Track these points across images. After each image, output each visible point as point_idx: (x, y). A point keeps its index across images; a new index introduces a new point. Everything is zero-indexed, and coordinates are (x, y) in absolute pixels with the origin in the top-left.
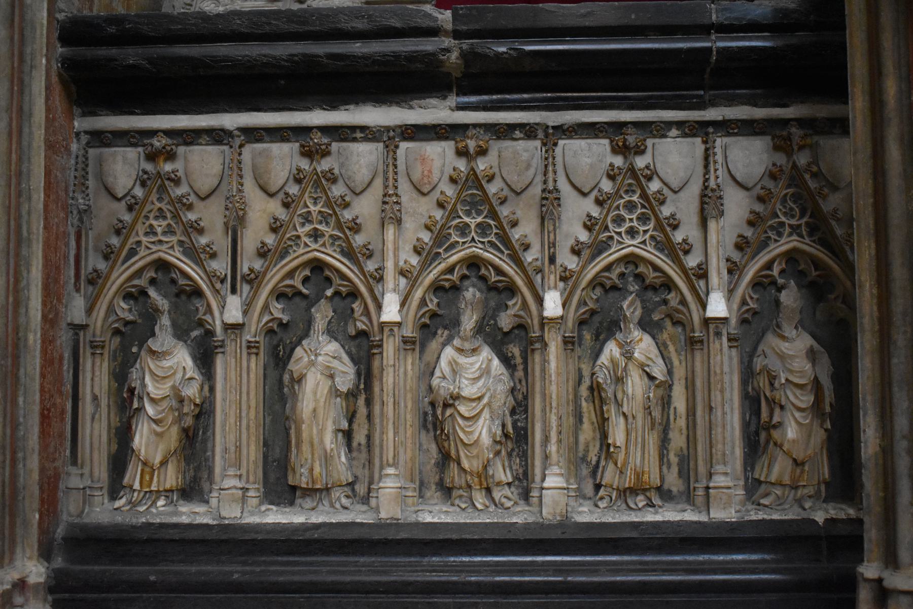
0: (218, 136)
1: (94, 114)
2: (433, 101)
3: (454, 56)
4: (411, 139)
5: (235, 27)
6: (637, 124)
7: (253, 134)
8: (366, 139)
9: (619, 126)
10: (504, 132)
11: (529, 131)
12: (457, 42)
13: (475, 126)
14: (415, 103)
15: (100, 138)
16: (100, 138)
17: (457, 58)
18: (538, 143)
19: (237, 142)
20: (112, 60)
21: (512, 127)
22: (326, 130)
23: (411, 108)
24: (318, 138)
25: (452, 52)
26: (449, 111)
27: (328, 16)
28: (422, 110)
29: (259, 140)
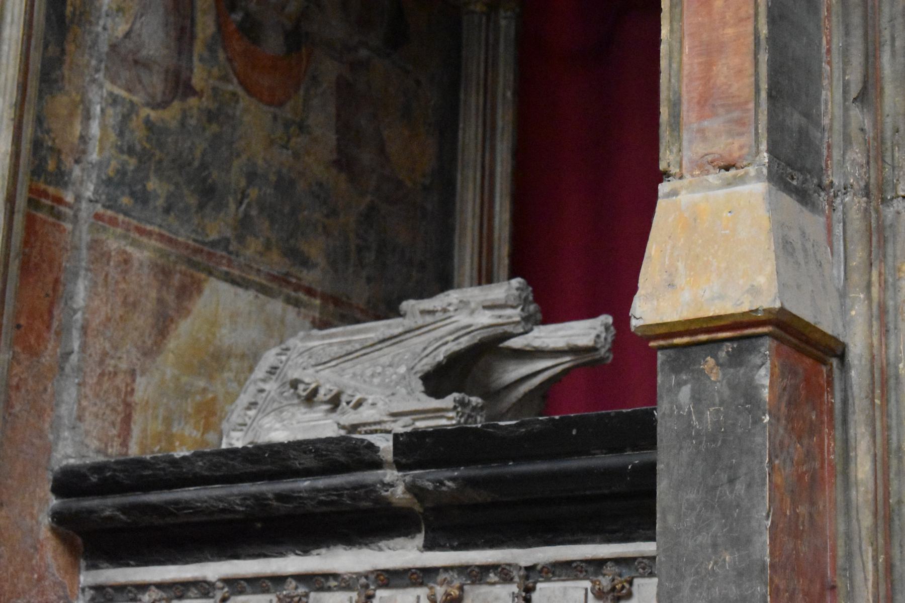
1: (95, 567)
2: (400, 541)
3: (400, 490)
4: (386, 585)
5: (197, 470)
6: (620, 561)
8: (340, 588)
9: (598, 564)
10: (478, 574)
11: (503, 573)
12: (401, 474)
13: (446, 569)
14: (382, 544)
17: (404, 493)
18: (514, 588)
19: (219, 595)
20: (91, 511)
21: (485, 569)
22: (303, 578)
23: (380, 549)
25: (395, 484)
26: (418, 553)
27: (278, 452)
28: (391, 552)
29: (241, 592)
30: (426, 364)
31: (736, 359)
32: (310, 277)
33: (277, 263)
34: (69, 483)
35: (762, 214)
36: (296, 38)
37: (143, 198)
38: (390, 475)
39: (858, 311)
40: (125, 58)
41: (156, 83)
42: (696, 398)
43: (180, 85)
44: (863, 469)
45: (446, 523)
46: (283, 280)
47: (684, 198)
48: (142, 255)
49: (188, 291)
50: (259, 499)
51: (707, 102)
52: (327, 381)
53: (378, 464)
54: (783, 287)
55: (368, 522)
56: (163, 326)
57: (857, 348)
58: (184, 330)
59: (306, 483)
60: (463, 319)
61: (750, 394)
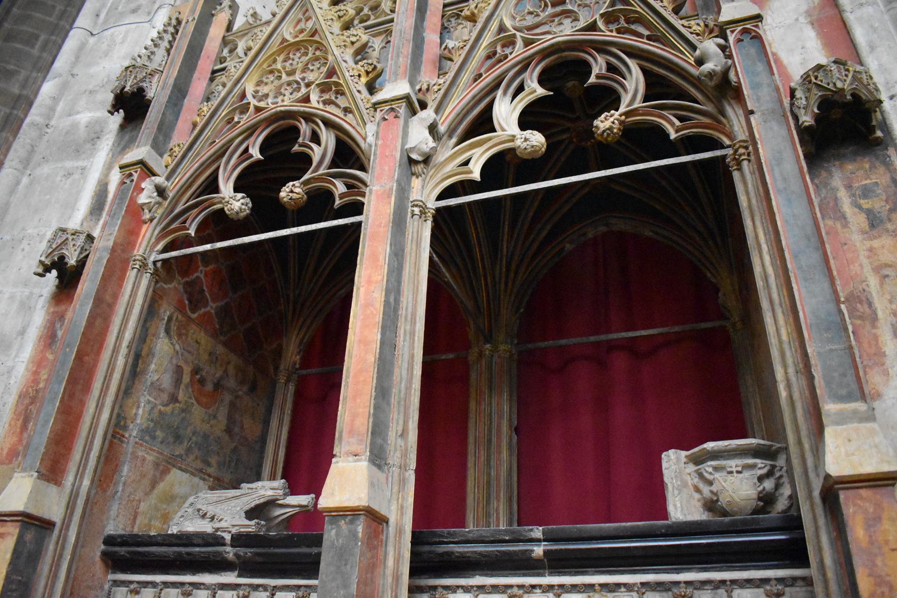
0: (154, 584)
1: (115, 573)
2: (229, 573)
4: (222, 589)
6: (306, 586)
7: (166, 584)
8: (205, 589)
9: (299, 587)
10: (256, 588)
11: (265, 588)
13: (245, 585)
15: (116, 583)
16: (116, 583)
18: (268, 594)
19: (160, 588)
20: (116, 552)
21: (258, 586)
22: (191, 584)
24: (188, 588)
25: (230, 552)
29: (168, 587)
30: (247, 507)
31: (352, 522)
32: (211, 470)
33: (199, 465)
34: (110, 541)
35: (365, 472)
36: (218, 386)
37: (154, 438)
38: (228, 549)
39: (394, 507)
40: (156, 387)
41: (165, 397)
42: (337, 535)
43: (174, 399)
44: (390, 562)
45: (247, 568)
46: (201, 471)
47: (340, 464)
48: (150, 458)
49: (166, 472)
50: (180, 553)
51: (351, 432)
52: (211, 510)
53: (224, 545)
54: (370, 498)
55: (218, 565)
56: (154, 484)
57: (392, 521)
58: (161, 486)
59: (198, 549)
60: (262, 492)
61: (354, 534)
